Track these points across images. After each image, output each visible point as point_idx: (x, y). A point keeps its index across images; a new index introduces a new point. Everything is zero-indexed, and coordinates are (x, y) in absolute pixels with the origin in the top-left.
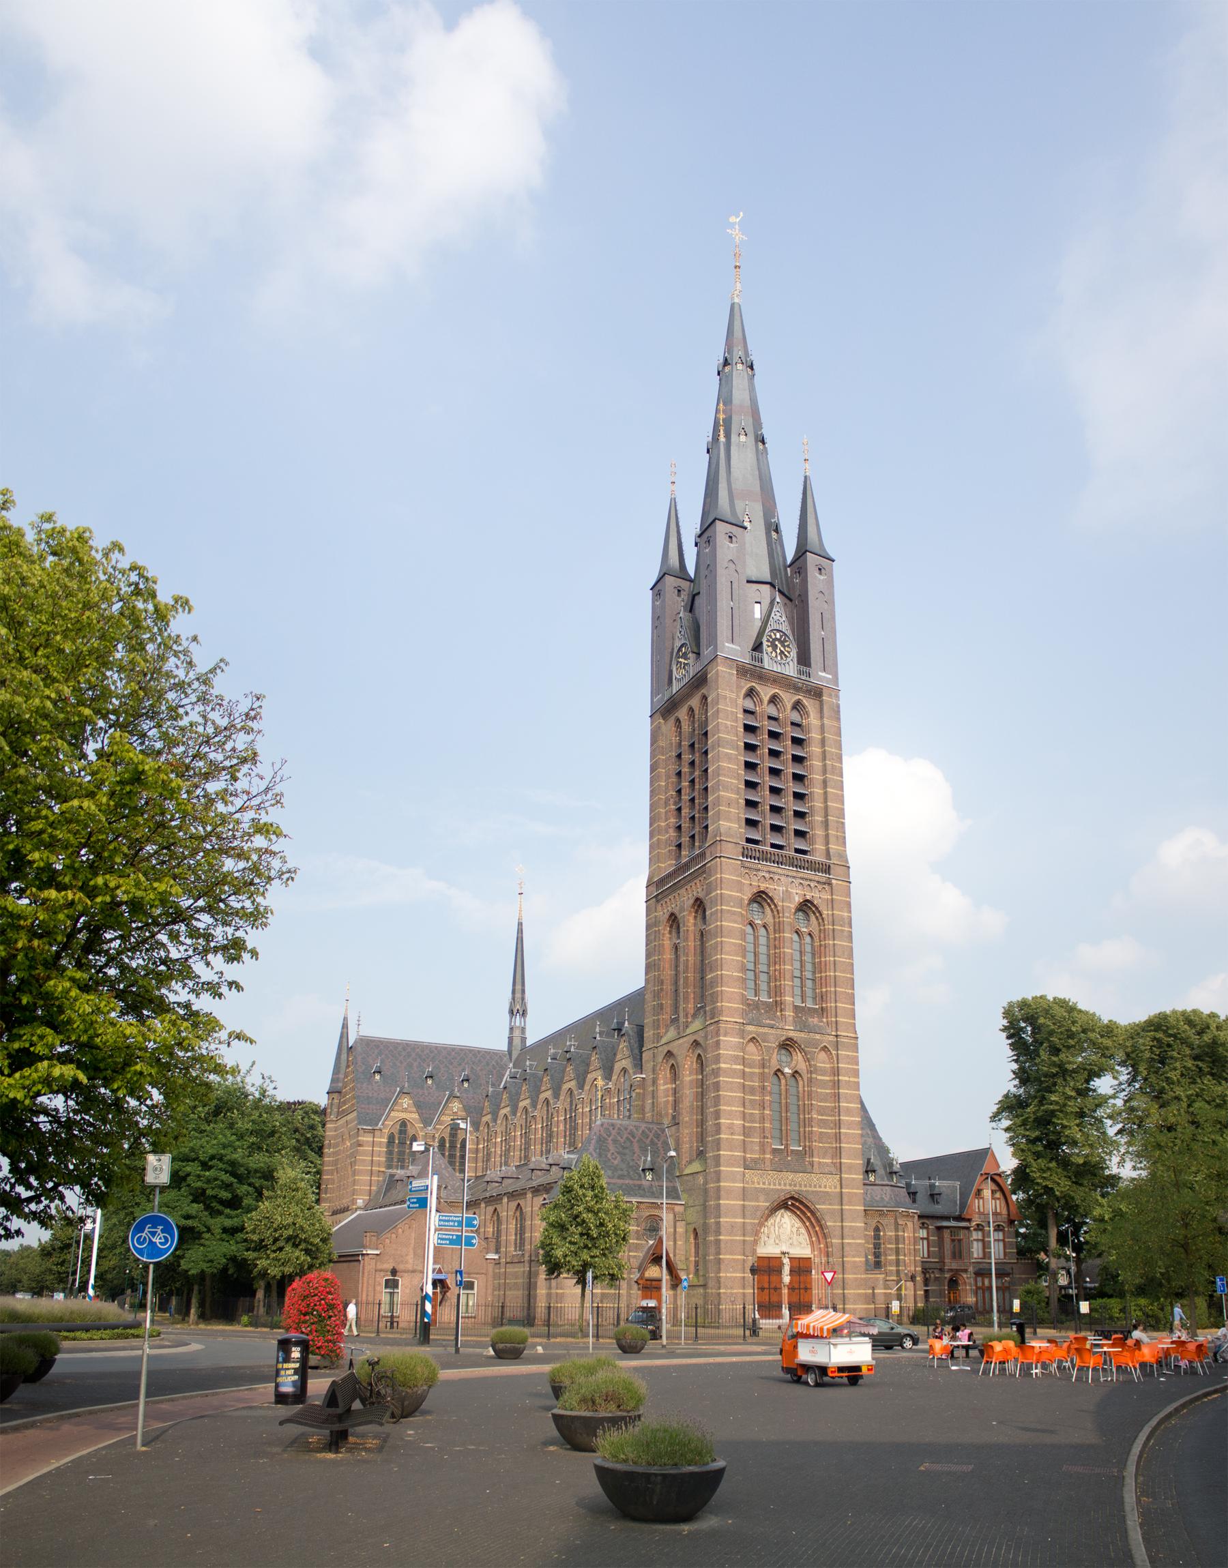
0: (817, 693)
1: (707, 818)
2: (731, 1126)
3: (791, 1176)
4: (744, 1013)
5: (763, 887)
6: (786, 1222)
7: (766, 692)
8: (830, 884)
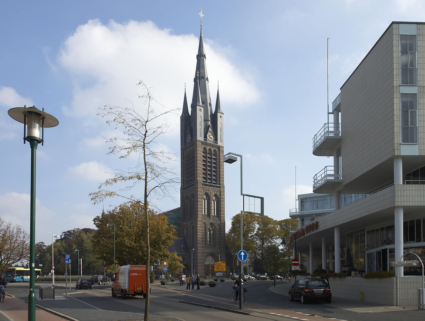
0: (219, 148)
6: (210, 258)
7: (208, 148)
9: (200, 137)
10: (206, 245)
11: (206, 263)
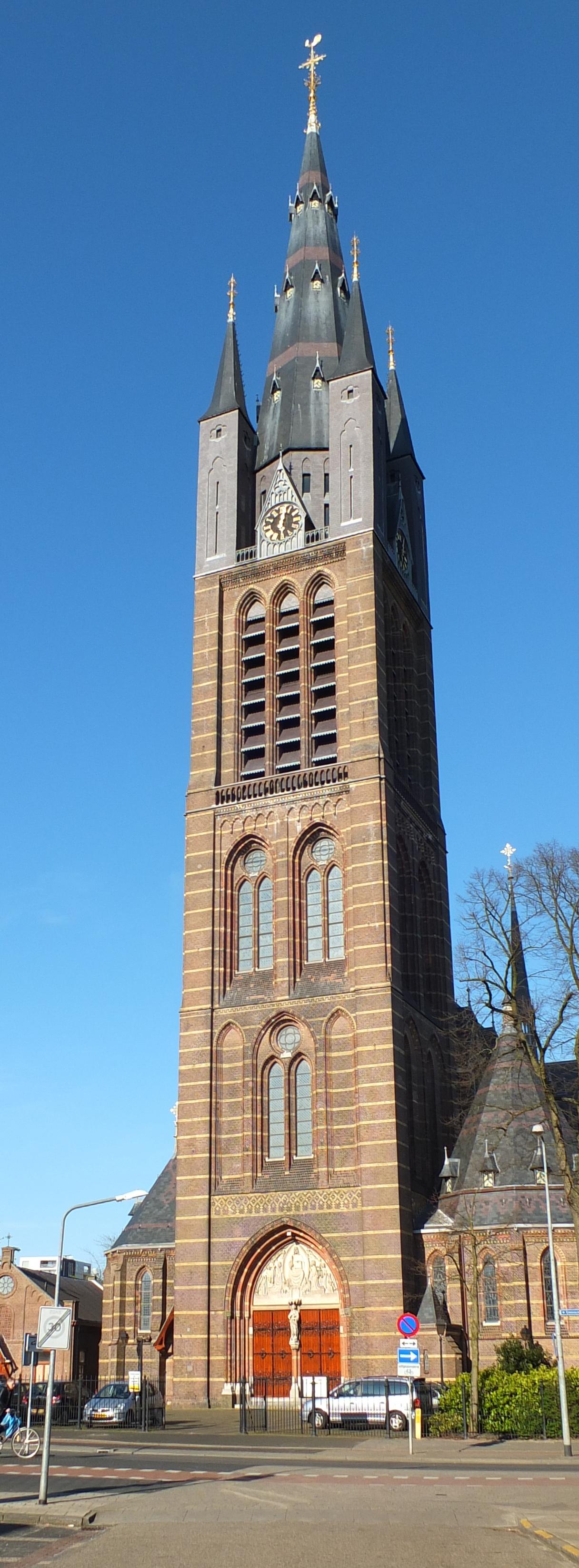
3: (282, 1196)
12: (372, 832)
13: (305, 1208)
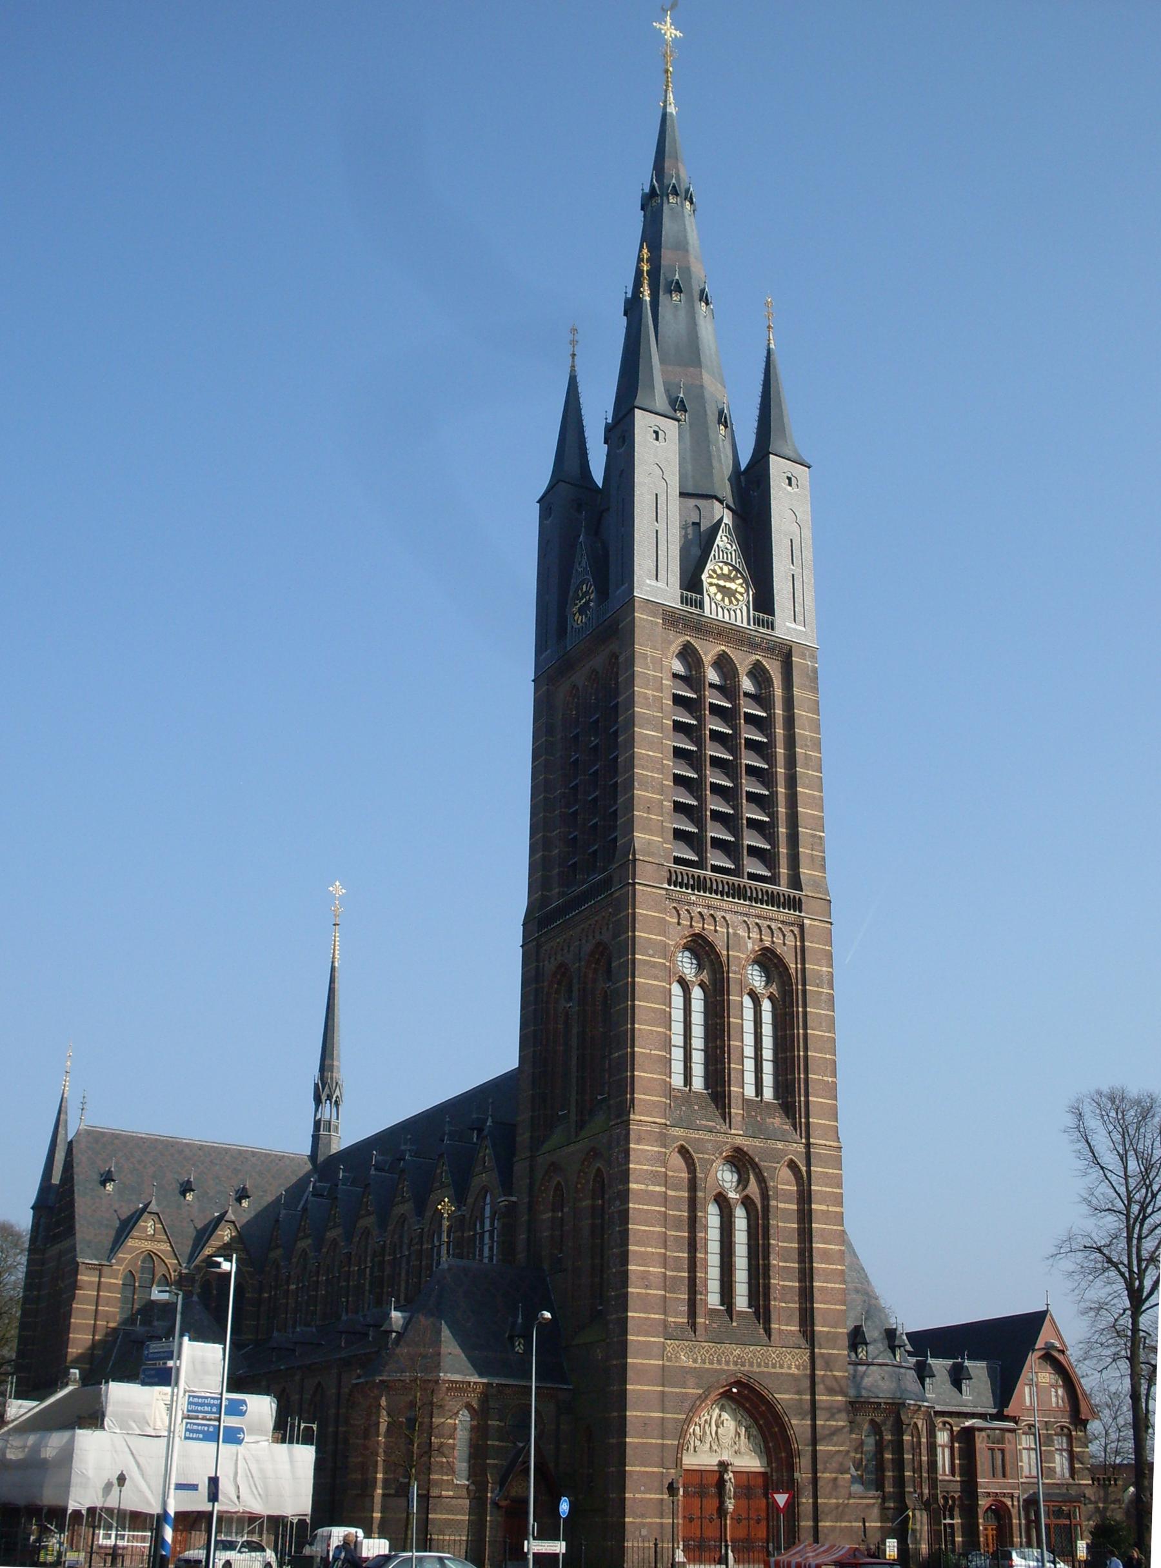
0: (786, 654)
1: (615, 828)
2: (645, 1276)
4: (666, 1110)
5: (697, 926)
7: (708, 651)
8: (802, 927)
9: (654, 581)
10: (692, 1313)
11: (690, 1461)
12: (825, 979)
13: (759, 1365)
